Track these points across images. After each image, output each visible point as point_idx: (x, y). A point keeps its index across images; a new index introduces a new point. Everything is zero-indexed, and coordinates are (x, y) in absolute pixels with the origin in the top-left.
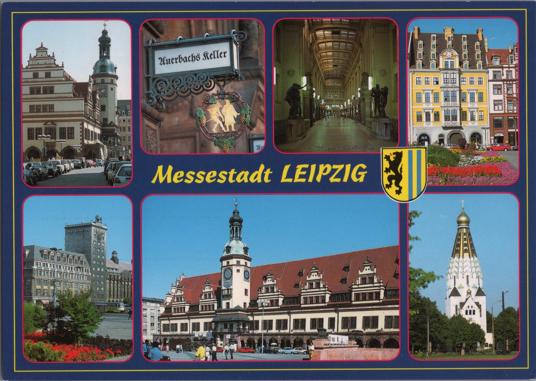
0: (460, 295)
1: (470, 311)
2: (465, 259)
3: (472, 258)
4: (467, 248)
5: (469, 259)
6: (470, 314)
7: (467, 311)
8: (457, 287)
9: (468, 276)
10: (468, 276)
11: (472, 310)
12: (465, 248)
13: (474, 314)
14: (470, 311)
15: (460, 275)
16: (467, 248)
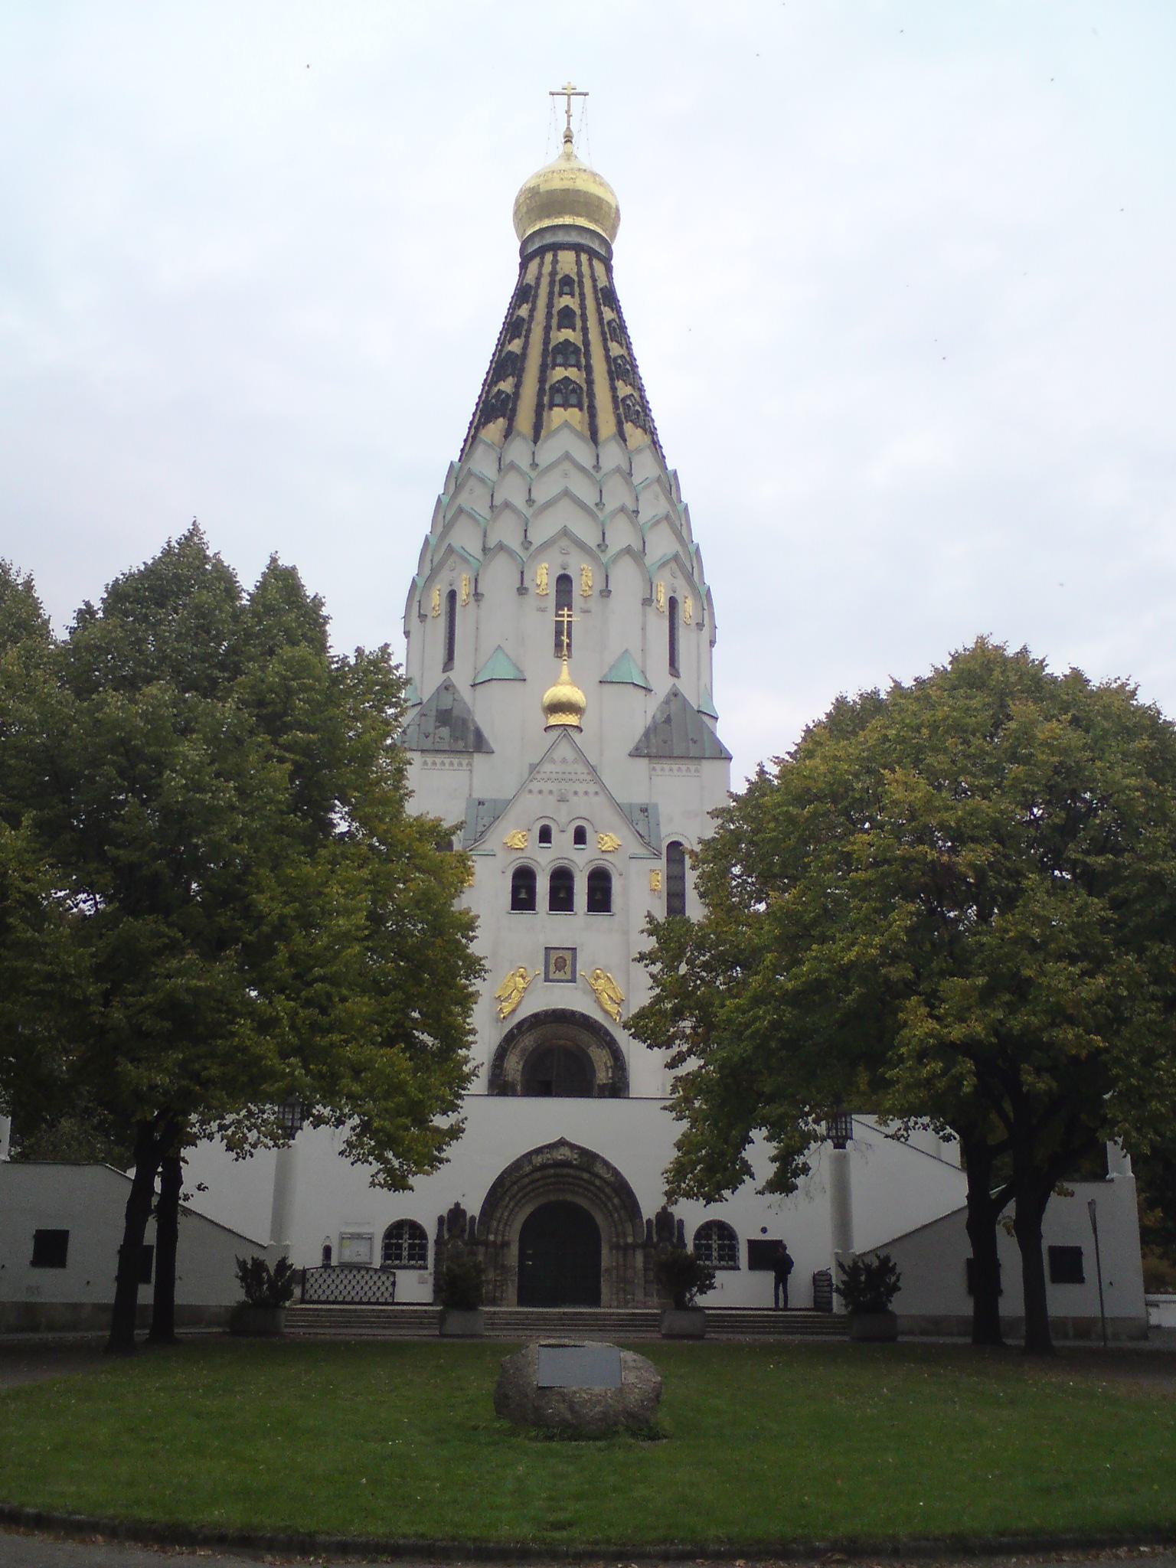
0: (479, 744)
1: (562, 879)
2: (549, 451)
3: (612, 455)
4: (572, 373)
5: (583, 453)
6: (561, 900)
7: (524, 878)
8: (461, 677)
9: (564, 582)
10: (564, 582)
11: (581, 863)
12: (559, 373)
13: (601, 898)
14: (562, 879)
15: (500, 576)
16: (572, 373)
